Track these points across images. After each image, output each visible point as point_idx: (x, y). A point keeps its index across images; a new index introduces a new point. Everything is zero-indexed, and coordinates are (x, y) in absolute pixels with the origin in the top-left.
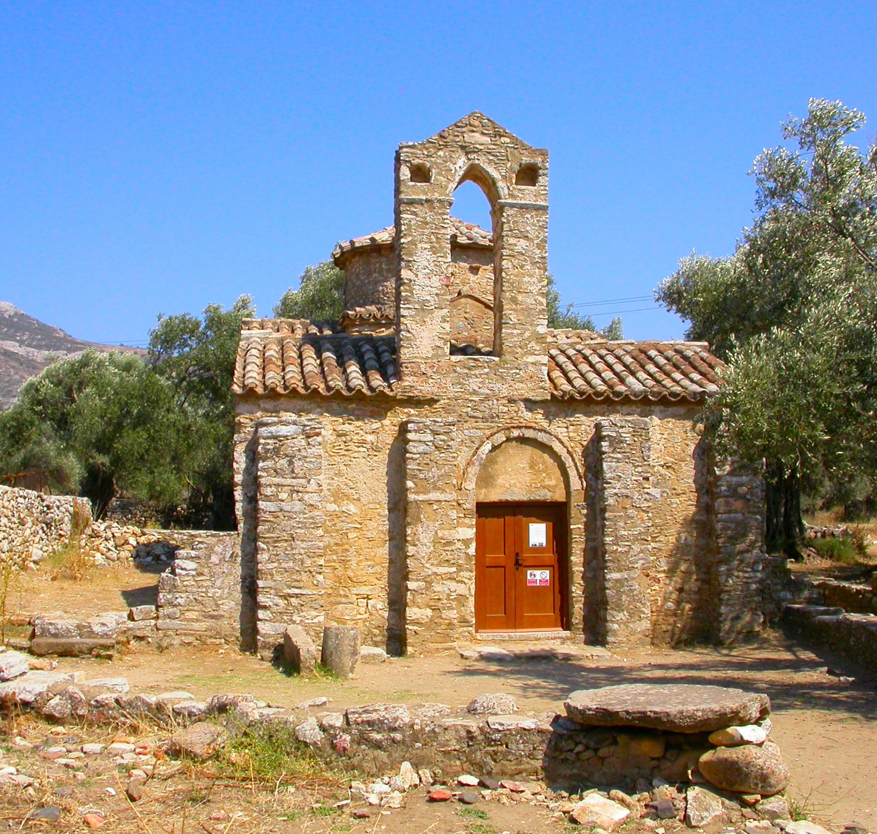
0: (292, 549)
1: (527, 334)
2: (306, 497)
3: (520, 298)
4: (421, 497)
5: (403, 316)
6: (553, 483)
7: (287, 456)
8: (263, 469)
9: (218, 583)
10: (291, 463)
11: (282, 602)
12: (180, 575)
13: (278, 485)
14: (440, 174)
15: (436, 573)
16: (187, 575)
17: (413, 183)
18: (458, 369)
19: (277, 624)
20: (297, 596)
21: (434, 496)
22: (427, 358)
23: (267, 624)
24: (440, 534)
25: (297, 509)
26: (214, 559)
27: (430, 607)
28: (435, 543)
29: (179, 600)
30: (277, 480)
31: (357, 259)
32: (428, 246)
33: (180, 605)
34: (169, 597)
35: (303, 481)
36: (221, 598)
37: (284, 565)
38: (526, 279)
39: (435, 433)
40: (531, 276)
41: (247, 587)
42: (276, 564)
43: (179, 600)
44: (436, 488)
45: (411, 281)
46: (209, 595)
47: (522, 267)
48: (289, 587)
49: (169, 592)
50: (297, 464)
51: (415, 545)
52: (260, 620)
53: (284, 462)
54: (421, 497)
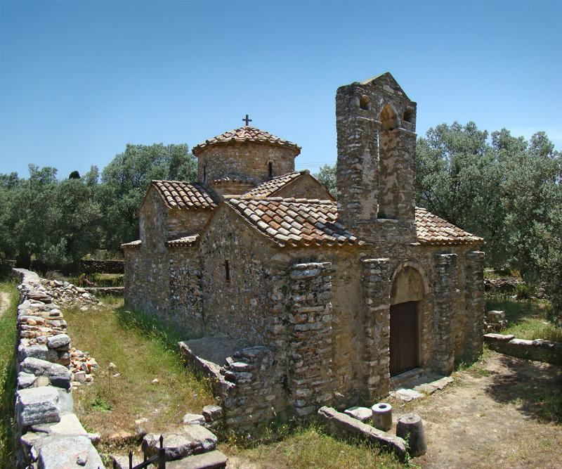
0: (316, 354)
1: (409, 207)
2: (324, 317)
3: (406, 186)
4: (376, 309)
5: (357, 193)
6: (417, 290)
7: (313, 291)
8: (299, 302)
9: (265, 385)
10: (315, 295)
11: (310, 392)
12: (242, 383)
13: (307, 313)
14: (372, 106)
15: (382, 354)
16: (246, 382)
17: (361, 109)
18: (383, 228)
19: (309, 407)
20: (318, 385)
21: (382, 307)
22: (368, 220)
23: (304, 409)
24: (384, 330)
25: (319, 327)
26: (263, 367)
27: (379, 374)
28: (381, 336)
29: (242, 402)
30: (308, 309)
31: (217, 149)
32: (368, 150)
33: (241, 404)
34: (235, 400)
35: (321, 307)
36: (267, 394)
37: (312, 367)
38: (409, 175)
39: (382, 269)
40: (410, 174)
41: (283, 383)
42: (307, 367)
43: (242, 402)
44: (382, 303)
45: (361, 171)
46: (261, 394)
47: (407, 168)
48: (314, 381)
49: (235, 397)
50: (319, 295)
51: (373, 339)
52: (299, 407)
53: (311, 296)
54: (376, 309)
